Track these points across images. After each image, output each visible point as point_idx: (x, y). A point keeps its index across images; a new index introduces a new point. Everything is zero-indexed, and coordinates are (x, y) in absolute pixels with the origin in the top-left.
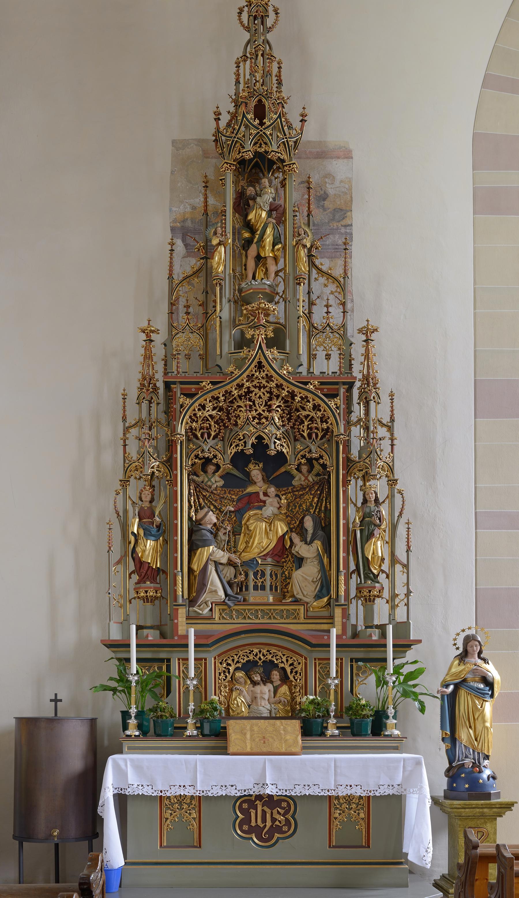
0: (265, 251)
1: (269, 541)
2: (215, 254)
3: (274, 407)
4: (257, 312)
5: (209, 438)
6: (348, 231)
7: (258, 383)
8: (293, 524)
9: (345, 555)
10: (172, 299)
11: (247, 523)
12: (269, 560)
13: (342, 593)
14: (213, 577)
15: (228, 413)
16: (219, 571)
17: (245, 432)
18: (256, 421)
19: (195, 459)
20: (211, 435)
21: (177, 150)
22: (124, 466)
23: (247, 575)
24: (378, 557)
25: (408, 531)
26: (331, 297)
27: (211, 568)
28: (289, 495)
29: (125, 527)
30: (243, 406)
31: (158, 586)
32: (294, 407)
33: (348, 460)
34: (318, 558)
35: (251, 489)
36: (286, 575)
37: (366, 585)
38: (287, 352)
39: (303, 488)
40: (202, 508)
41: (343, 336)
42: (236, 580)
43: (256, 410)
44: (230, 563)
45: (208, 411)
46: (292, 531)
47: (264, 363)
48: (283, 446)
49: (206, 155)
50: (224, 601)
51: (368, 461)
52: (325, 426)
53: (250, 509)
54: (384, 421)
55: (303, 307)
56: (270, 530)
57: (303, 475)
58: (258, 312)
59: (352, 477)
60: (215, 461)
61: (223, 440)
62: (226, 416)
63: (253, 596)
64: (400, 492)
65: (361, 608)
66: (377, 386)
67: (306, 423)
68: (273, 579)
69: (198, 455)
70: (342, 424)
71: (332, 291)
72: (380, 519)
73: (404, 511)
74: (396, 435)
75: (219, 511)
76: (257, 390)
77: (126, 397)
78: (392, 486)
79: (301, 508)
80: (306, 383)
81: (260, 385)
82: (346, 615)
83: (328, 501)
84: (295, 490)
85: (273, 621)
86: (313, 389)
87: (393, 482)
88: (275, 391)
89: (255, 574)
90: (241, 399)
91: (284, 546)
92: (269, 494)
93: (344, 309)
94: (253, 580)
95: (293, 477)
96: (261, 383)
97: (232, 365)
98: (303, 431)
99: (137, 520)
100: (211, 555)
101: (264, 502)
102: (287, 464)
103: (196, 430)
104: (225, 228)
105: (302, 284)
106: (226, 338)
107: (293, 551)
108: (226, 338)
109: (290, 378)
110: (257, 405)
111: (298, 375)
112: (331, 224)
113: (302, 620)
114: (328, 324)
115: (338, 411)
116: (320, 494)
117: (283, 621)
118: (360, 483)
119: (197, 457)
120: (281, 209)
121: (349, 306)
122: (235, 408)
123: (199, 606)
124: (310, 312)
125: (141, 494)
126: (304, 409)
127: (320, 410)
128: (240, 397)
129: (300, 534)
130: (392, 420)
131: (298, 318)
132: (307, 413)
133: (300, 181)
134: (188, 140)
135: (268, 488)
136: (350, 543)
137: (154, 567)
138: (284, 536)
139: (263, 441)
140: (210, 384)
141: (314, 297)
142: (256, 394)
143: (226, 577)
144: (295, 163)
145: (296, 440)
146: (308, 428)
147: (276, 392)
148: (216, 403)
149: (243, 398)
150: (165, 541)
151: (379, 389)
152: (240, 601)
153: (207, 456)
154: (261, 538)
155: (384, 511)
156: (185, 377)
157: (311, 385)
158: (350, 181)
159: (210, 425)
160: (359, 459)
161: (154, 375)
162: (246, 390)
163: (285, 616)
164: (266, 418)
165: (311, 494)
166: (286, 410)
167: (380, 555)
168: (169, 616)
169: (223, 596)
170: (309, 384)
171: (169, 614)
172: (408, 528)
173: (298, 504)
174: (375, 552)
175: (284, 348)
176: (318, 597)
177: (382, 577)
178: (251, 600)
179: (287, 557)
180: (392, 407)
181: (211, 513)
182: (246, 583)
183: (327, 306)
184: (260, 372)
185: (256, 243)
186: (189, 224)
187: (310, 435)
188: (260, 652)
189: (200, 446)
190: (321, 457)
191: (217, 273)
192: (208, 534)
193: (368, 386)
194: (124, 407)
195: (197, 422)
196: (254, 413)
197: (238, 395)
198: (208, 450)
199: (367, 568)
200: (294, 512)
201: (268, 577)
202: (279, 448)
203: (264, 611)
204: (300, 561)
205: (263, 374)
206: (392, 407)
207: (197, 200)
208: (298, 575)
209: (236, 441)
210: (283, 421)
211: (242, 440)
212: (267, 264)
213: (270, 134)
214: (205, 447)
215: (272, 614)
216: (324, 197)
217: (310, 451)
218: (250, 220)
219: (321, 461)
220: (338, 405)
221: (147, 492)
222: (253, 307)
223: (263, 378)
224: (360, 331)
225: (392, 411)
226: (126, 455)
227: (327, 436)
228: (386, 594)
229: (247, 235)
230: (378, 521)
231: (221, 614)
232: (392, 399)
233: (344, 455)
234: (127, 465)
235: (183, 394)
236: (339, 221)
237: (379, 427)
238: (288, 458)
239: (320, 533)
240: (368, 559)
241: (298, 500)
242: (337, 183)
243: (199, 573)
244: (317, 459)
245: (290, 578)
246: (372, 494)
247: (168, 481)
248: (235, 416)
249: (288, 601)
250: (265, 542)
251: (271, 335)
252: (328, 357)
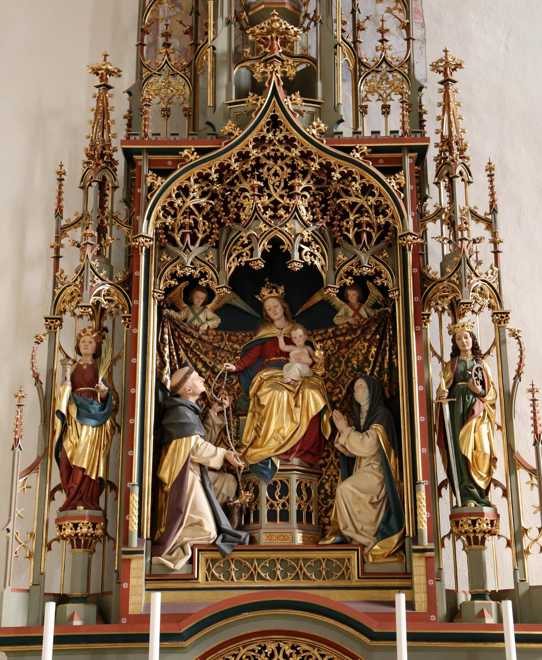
1: (295, 426)
3: (298, 190)
4: (269, 37)
5: (193, 243)
7: (273, 150)
8: (337, 395)
9: (425, 450)
11: (259, 393)
12: (295, 461)
13: (424, 527)
14: (196, 494)
15: (226, 202)
16: (207, 483)
17: (252, 232)
18: (270, 213)
19: (171, 279)
20: (197, 238)
22: (54, 293)
23: (257, 492)
24: (485, 454)
25: (534, 406)
26: (386, 15)
27: (193, 477)
28: (329, 342)
29: (47, 400)
30: (248, 188)
31: (99, 513)
32: (331, 190)
33: (423, 280)
34: (379, 456)
35: (264, 333)
36: (326, 490)
37: (466, 510)
38: (319, 100)
39: (351, 329)
40: (181, 366)
41: (409, 78)
42: (238, 501)
43: (270, 196)
44: (227, 467)
45: (194, 198)
46: (334, 408)
47: (282, 118)
48: (315, 256)
50: (214, 544)
51: (455, 279)
52: (382, 220)
53: (263, 368)
54: (481, 213)
56: (296, 405)
57: (351, 307)
59: (433, 310)
60: (203, 282)
61: (217, 247)
62: (222, 206)
63: (268, 533)
64: (514, 334)
65: (462, 557)
66: (466, 154)
67: (352, 217)
68: (302, 499)
69: (176, 272)
70: (410, 216)
71: (389, 8)
72: (483, 383)
73: (524, 369)
74: (501, 235)
75: (209, 372)
76: (271, 162)
77: (63, 176)
78: (500, 323)
79: (350, 365)
80: (348, 150)
81: (276, 154)
82: (434, 573)
83: (393, 352)
84: (338, 333)
85: (303, 583)
86: (361, 158)
87: (502, 317)
88: (301, 164)
89: (271, 489)
90: (246, 178)
91: (321, 435)
92: (295, 341)
94: (268, 501)
95: (335, 311)
96: (278, 150)
97: (230, 122)
98: (348, 230)
99: (69, 388)
100: (193, 452)
101: (287, 355)
102: (323, 288)
103: (173, 230)
107: (336, 445)
109: (323, 142)
110: (271, 187)
111: (336, 137)
113: (355, 581)
114: (384, 59)
115: (402, 195)
116: (381, 340)
117: (320, 583)
118: (447, 319)
119: (173, 276)
121: (416, 32)
122: (237, 194)
123: (170, 553)
124: (356, 41)
125: (78, 342)
126: (347, 193)
127: (373, 195)
128: (244, 174)
129: (349, 412)
130: (493, 210)
131: (336, 47)
132: (354, 199)
135: (292, 330)
136: (435, 430)
137: (93, 477)
138: (320, 415)
139: (281, 247)
140: (195, 153)
142: (269, 170)
143: (220, 496)
145: (336, 246)
146: (356, 225)
147: (303, 165)
148: (207, 185)
149: (249, 176)
150: (115, 427)
151: (468, 159)
152: (243, 543)
153: (188, 274)
154: (281, 420)
155: (490, 366)
156: (156, 142)
157: (357, 152)
159: (196, 222)
160: (441, 276)
161: (110, 140)
162: (254, 163)
163: (324, 572)
164: (286, 208)
165: (365, 341)
166: (319, 194)
167: (488, 451)
168: (115, 575)
169: (214, 533)
170: (354, 151)
171: (117, 571)
172: (534, 400)
173: (343, 358)
174: (479, 445)
175: (315, 96)
176: (382, 533)
177: (495, 495)
178: (263, 540)
179: (328, 456)
180: (492, 188)
181: (195, 374)
182: (256, 507)
183: (382, 31)
184: (275, 132)
187: (358, 237)
188: (279, 648)
189: (179, 257)
190: (378, 274)
192: (190, 414)
193: (451, 154)
194: (60, 193)
195: (174, 216)
196: (266, 200)
197: (242, 171)
198: (192, 263)
199: (465, 477)
200: (337, 373)
201: (293, 494)
202: (308, 259)
203: (287, 562)
204: (348, 464)
205: (280, 136)
206: (492, 188)
208: (346, 490)
209: (238, 248)
210: (313, 214)
211: (247, 245)
214: (186, 259)
215: (301, 569)
217: (359, 265)
219: (379, 281)
220: (402, 186)
221: (88, 338)
223: (280, 142)
224: (435, 67)
225: (492, 195)
226: (58, 274)
227: (386, 238)
228: (504, 528)
230: (480, 388)
231: (209, 569)
232: (491, 176)
233: (416, 270)
234: (58, 292)
235: (152, 170)
237: (472, 223)
238: (324, 276)
239: (381, 410)
240: (466, 459)
241: (343, 350)
243: (172, 487)
244: (371, 278)
245: (333, 496)
246: (466, 338)
247: (124, 318)
248: (236, 206)
249: (328, 542)
250: (287, 429)
252: (386, 110)
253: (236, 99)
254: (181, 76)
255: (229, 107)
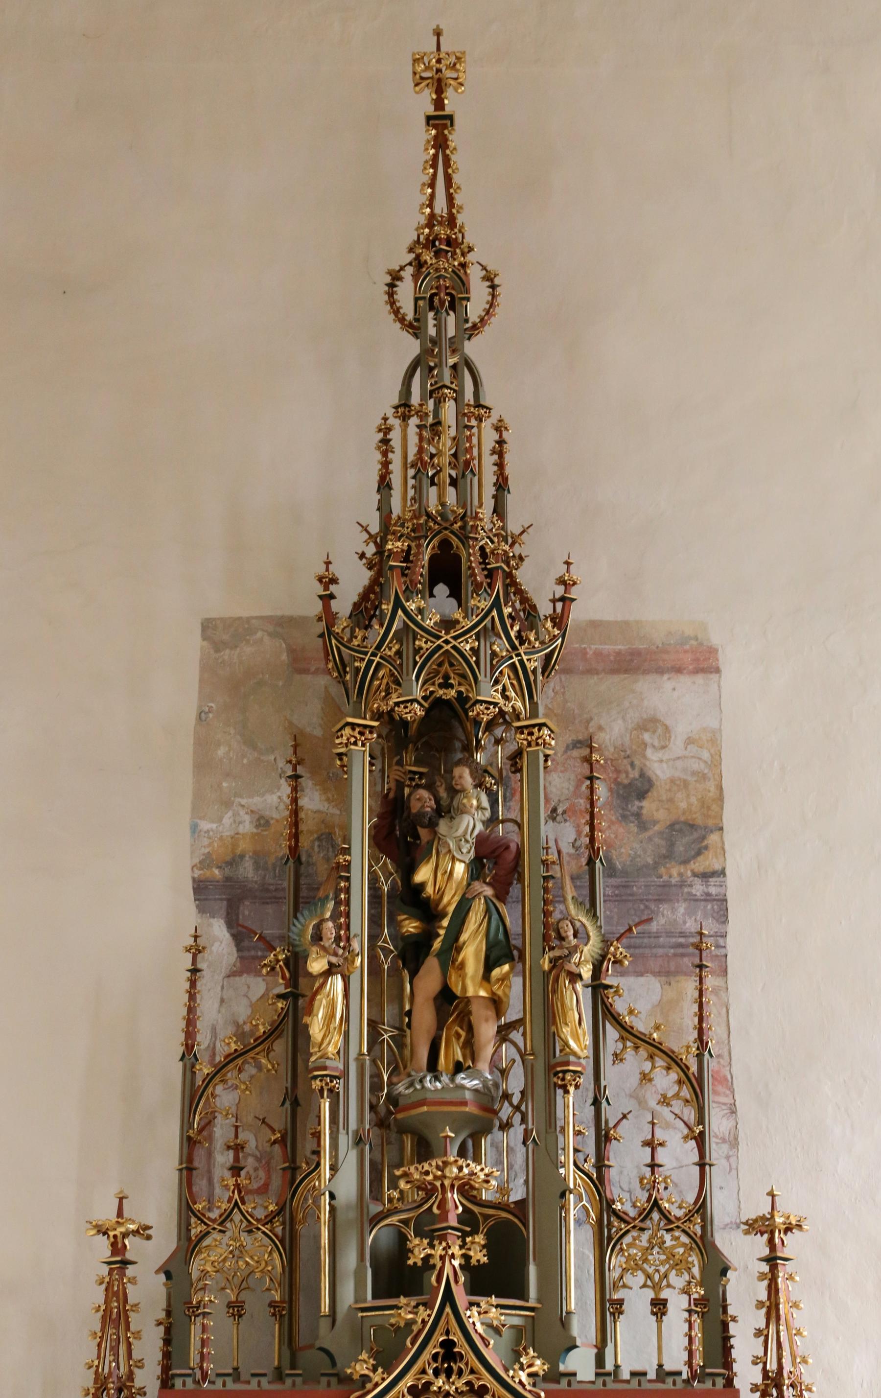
0: (463, 977)
2: (316, 1003)
6: (713, 890)
10: (191, 1126)
21: (217, 651)
38: (532, 1303)
49: (298, 664)
55: (576, 1151)
58: (442, 1185)
93: (702, 1155)
104: (348, 915)
105: (572, 1089)
106: (350, 1260)
108: (350, 1260)
112: (662, 870)
120: (510, 856)
133: (569, 741)
134: (248, 620)
141: (610, 1114)
144: (544, 725)
158: (714, 740)
175: (522, 1294)
185: (438, 955)
186: (247, 871)
191: (325, 1056)
207: (272, 799)
212: (470, 1013)
213: (472, 649)
216: (637, 788)
218: (422, 886)
222: (427, 1173)
229: (411, 926)
236: (686, 862)
242: (677, 746)
251: (479, 1256)
253: (374, 1297)
254: (264, 1233)
255: (360, 1314)
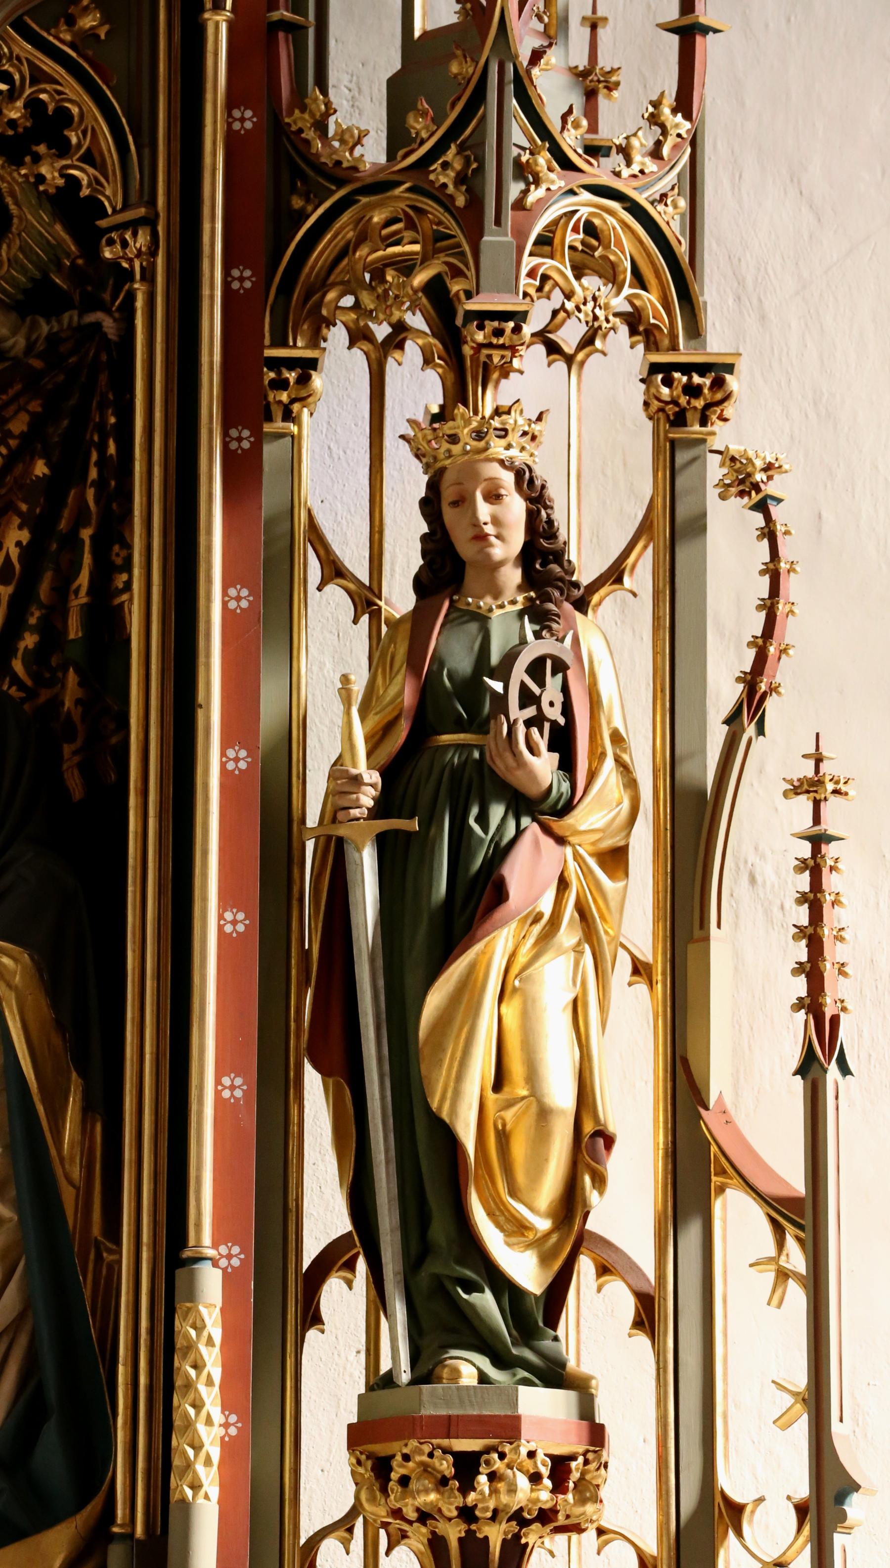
25: (814, 868)
64: (745, 482)
72: (562, 741)
73: (783, 673)
87: (693, 391)
172: (818, 841)
